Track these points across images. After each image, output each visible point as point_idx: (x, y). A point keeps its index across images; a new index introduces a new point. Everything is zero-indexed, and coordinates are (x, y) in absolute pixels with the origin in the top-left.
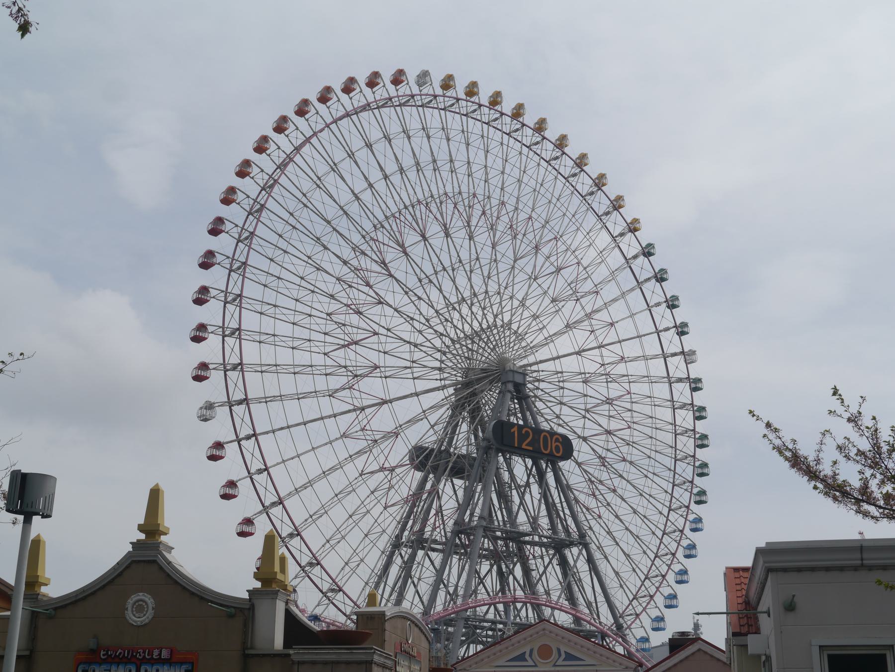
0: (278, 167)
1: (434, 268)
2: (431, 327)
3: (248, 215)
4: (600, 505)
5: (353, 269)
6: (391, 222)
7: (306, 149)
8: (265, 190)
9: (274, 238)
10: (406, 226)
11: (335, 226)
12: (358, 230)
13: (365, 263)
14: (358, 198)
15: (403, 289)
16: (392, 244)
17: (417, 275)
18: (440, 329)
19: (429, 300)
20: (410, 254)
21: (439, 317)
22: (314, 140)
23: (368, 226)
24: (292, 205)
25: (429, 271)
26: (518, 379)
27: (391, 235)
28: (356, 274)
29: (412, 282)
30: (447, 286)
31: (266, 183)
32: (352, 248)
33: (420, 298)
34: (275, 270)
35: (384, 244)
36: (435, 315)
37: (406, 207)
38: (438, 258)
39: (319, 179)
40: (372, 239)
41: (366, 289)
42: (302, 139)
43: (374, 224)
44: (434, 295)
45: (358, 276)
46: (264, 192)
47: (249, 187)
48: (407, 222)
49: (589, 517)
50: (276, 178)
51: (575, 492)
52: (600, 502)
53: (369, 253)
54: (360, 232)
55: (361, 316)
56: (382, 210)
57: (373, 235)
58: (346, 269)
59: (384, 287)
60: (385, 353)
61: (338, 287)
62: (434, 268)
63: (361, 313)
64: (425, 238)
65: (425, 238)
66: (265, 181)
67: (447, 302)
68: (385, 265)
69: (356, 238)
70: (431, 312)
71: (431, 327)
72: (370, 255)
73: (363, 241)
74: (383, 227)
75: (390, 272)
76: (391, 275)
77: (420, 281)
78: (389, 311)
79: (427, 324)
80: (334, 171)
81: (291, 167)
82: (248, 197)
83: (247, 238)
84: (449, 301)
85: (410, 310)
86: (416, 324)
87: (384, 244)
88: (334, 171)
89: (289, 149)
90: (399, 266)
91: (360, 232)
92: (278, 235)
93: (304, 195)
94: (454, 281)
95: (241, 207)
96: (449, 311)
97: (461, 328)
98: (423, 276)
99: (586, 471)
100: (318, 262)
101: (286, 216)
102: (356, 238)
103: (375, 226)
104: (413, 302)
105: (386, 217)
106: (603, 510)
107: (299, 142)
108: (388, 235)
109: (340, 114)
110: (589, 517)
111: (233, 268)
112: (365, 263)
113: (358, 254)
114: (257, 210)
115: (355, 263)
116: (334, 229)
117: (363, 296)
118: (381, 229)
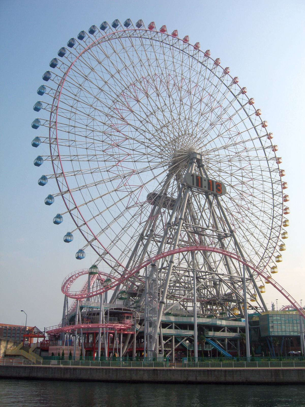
0: (59, 85)
1: (146, 114)
2: (153, 143)
3: (51, 113)
4: (247, 203)
5: (110, 126)
6: (121, 98)
7: (71, 73)
8: (56, 98)
9: (67, 122)
10: (128, 97)
11: (95, 107)
12: (106, 106)
13: (114, 121)
14: (102, 90)
15: (134, 128)
16: (124, 108)
17: (139, 120)
18: (157, 143)
19: (148, 130)
20: (134, 111)
21: (155, 138)
22: (73, 67)
23: (110, 103)
24: (71, 102)
25: (145, 116)
26: (198, 157)
27: (122, 104)
28: (112, 128)
29: (138, 124)
30: (155, 121)
31: (56, 95)
32: (106, 115)
33: (145, 131)
34: (72, 137)
35: (120, 109)
36: (152, 137)
37: (126, 89)
38: (147, 109)
39: (80, 85)
40: (114, 108)
41: (117, 134)
42: (67, 68)
43: (113, 101)
44: (150, 127)
45: (113, 129)
46: (56, 100)
47: (47, 99)
48: (128, 96)
49: (244, 210)
50: (60, 91)
51: (236, 201)
52: (247, 202)
53: (115, 115)
54: (107, 107)
55: (119, 147)
56: (114, 93)
57: (114, 106)
58: (106, 127)
59: (128, 131)
60: (135, 162)
61: (105, 137)
62: (146, 114)
63: (118, 146)
64: (138, 101)
65: (138, 101)
66: (55, 94)
67: (156, 128)
68: (123, 119)
69: (106, 110)
70: (150, 135)
71: (153, 143)
72: (116, 117)
73: (110, 111)
74: (118, 101)
75: (127, 122)
76: (128, 124)
77: (141, 122)
78: (132, 141)
79: (150, 142)
80: (87, 80)
81: (65, 84)
82: (49, 104)
83: (53, 125)
84: (157, 128)
85: (141, 138)
86: (146, 144)
87: (120, 109)
88: (87, 80)
89: (62, 75)
90: (130, 118)
91: (107, 107)
92: (69, 119)
93: (76, 95)
94: (158, 119)
95: (47, 110)
96: (159, 134)
97: (166, 140)
98: (142, 119)
99: (238, 190)
100: (92, 127)
101: (70, 109)
102: (106, 110)
103: (113, 102)
104: (141, 134)
105: (118, 96)
106: (249, 205)
107: (66, 70)
108: (121, 104)
109: (82, 51)
110: (244, 210)
111: (51, 142)
112: (114, 121)
113: (109, 118)
114: (54, 110)
115: (109, 122)
116: (95, 109)
117: (117, 138)
118: (118, 103)
